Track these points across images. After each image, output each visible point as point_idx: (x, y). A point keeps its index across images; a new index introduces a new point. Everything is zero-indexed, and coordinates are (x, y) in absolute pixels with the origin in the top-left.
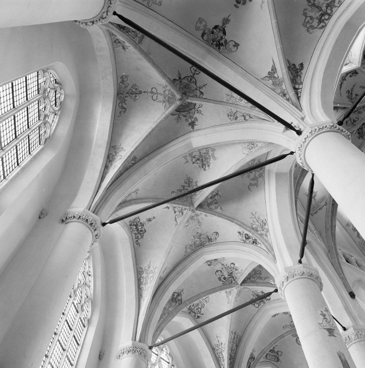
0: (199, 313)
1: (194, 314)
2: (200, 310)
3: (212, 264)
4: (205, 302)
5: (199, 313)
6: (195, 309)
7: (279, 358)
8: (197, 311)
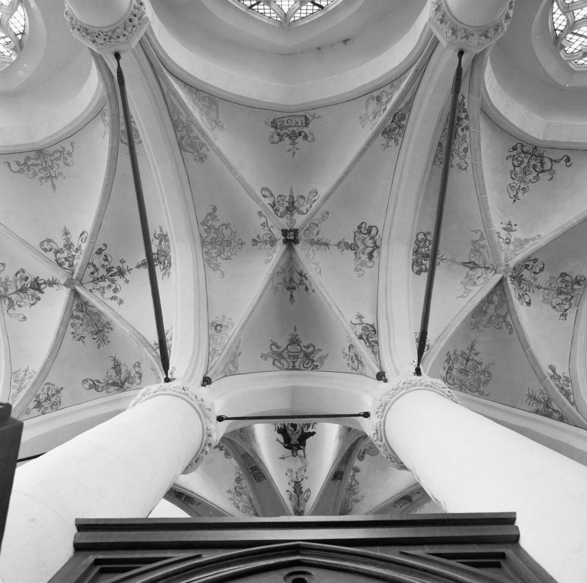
0: (516, 157)
1: (524, 150)
2: (516, 163)
3: (560, 279)
4: (514, 185)
5: (516, 157)
6: (526, 161)
7: (273, 130)
8: (520, 159)
